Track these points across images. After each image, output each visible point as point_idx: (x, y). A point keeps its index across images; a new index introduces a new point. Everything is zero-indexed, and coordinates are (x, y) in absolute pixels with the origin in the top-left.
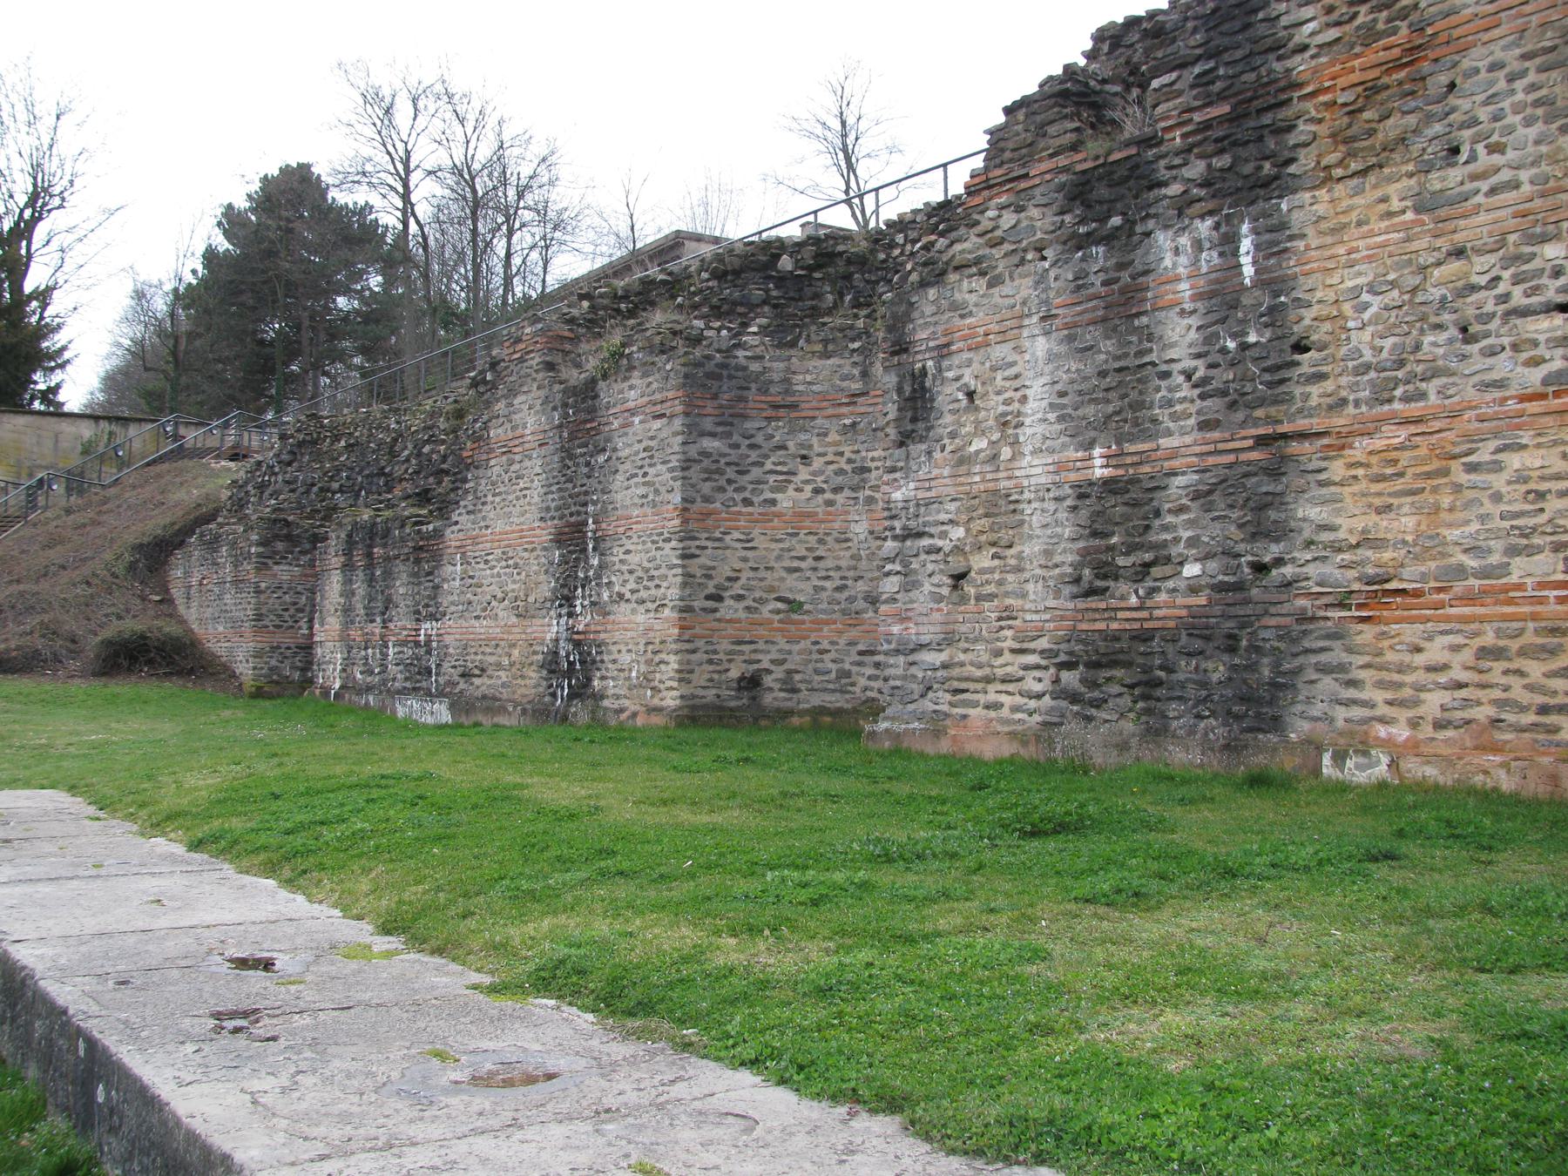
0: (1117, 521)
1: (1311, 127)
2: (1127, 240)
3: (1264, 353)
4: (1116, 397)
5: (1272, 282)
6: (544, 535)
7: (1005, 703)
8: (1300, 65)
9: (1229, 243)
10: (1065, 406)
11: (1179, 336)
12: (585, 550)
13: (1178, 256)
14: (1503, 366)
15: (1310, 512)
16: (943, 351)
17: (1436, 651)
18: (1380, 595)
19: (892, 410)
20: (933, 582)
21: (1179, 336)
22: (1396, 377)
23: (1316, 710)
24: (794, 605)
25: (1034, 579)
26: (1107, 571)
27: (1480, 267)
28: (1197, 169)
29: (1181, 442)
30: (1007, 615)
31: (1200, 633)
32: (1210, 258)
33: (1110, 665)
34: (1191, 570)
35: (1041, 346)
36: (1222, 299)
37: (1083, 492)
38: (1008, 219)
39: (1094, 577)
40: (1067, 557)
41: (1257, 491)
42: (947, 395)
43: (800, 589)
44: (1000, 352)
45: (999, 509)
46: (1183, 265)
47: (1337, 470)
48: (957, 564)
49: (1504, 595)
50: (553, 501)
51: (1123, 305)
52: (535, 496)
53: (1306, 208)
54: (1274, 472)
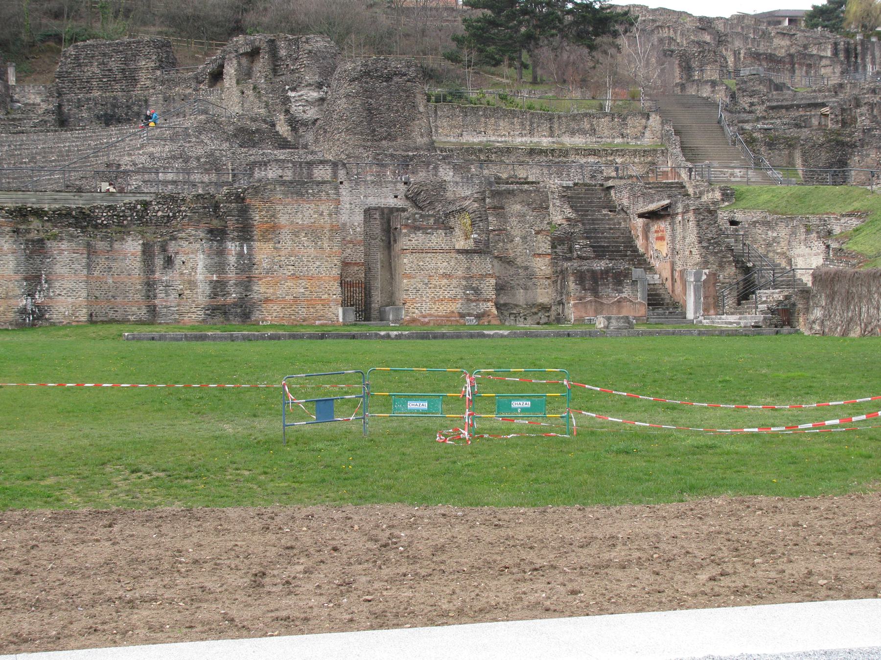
0: (218, 287)
1: (256, 233)
2: (221, 241)
3: (247, 265)
4: (220, 267)
5: (250, 254)
6: (19, 277)
7: (194, 315)
8: (255, 223)
9: (242, 247)
10: (208, 269)
11: (232, 259)
12: (40, 282)
13: (232, 247)
14: (285, 272)
15: (255, 288)
16: (177, 253)
17: (275, 308)
18: (267, 300)
19: (162, 263)
20: (173, 295)
21: (232, 259)
22: (269, 271)
23: (256, 315)
24: (97, 298)
25: (202, 294)
26: (216, 295)
27: (283, 258)
28: (236, 234)
29: (232, 276)
30: (194, 301)
31: (235, 305)
32: (238, 248)
33: (217, 311)
34: (234, 295)
35: (202, 256)
36: (240, 255)
37: (211, 282)
38: (193, 232)
39: (214, 295)
40: (208, 292)
41: (247, 284)
42: (178, 261)
43: (98, 294)
44: (191, 256)
45: (192, 284)
46: (233, 248)
47: (260, 282)
48: (180, 292)
49: (285, 301)
50: (22, 268)
51: (221, 253)
52: (12, 265)
53: (256, 245)
54: (249, 282)
